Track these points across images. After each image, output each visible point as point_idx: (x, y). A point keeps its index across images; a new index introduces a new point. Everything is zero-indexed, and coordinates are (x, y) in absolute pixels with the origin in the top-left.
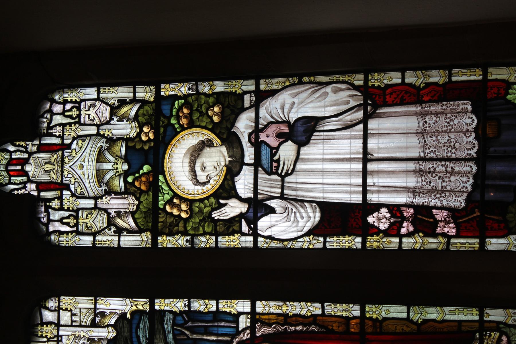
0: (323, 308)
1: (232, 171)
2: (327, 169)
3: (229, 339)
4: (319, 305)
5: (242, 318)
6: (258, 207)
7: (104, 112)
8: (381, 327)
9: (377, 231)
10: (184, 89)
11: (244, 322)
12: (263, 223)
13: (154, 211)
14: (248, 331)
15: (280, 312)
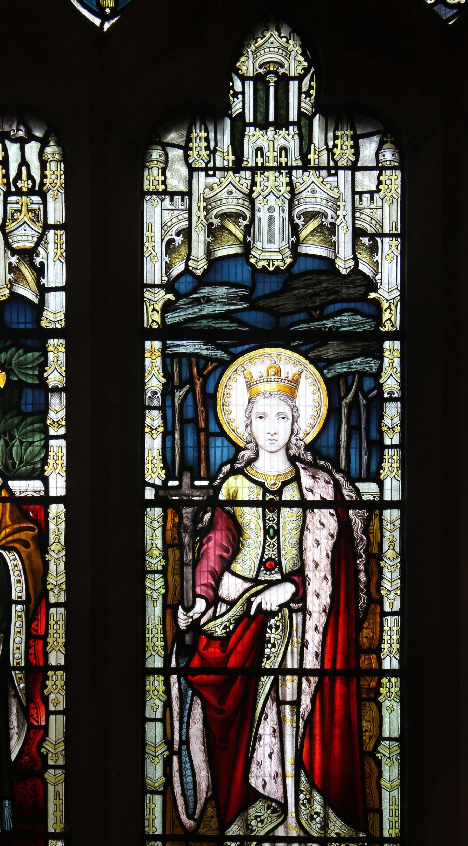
0: (392, 614)
3: (343, 465)
4: (397, 607)
5: (373, 487)
8: (369, 700)
11: (368, 490)
14: (354, 496)
15: (386, 547)
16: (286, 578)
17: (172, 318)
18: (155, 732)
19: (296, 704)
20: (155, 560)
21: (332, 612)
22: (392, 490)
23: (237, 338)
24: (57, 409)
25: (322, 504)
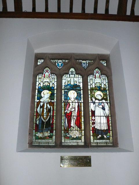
1: (98, 100)
2: (99, 111)
6: (94, 103)
7: (105, 83)
9: (92, 118)
10: (108, 94)
11: (80, 101)
12: (92, 104)
13: (93, 90)
16: (74, 108)
17: (65, 88)
18: (63, 121)
19: (75, 119)
20: (63, 107)
21: (78, 111)
22: (82, 101)
23: (69, 90)
24: (55, 95)
25: (77, 102)
